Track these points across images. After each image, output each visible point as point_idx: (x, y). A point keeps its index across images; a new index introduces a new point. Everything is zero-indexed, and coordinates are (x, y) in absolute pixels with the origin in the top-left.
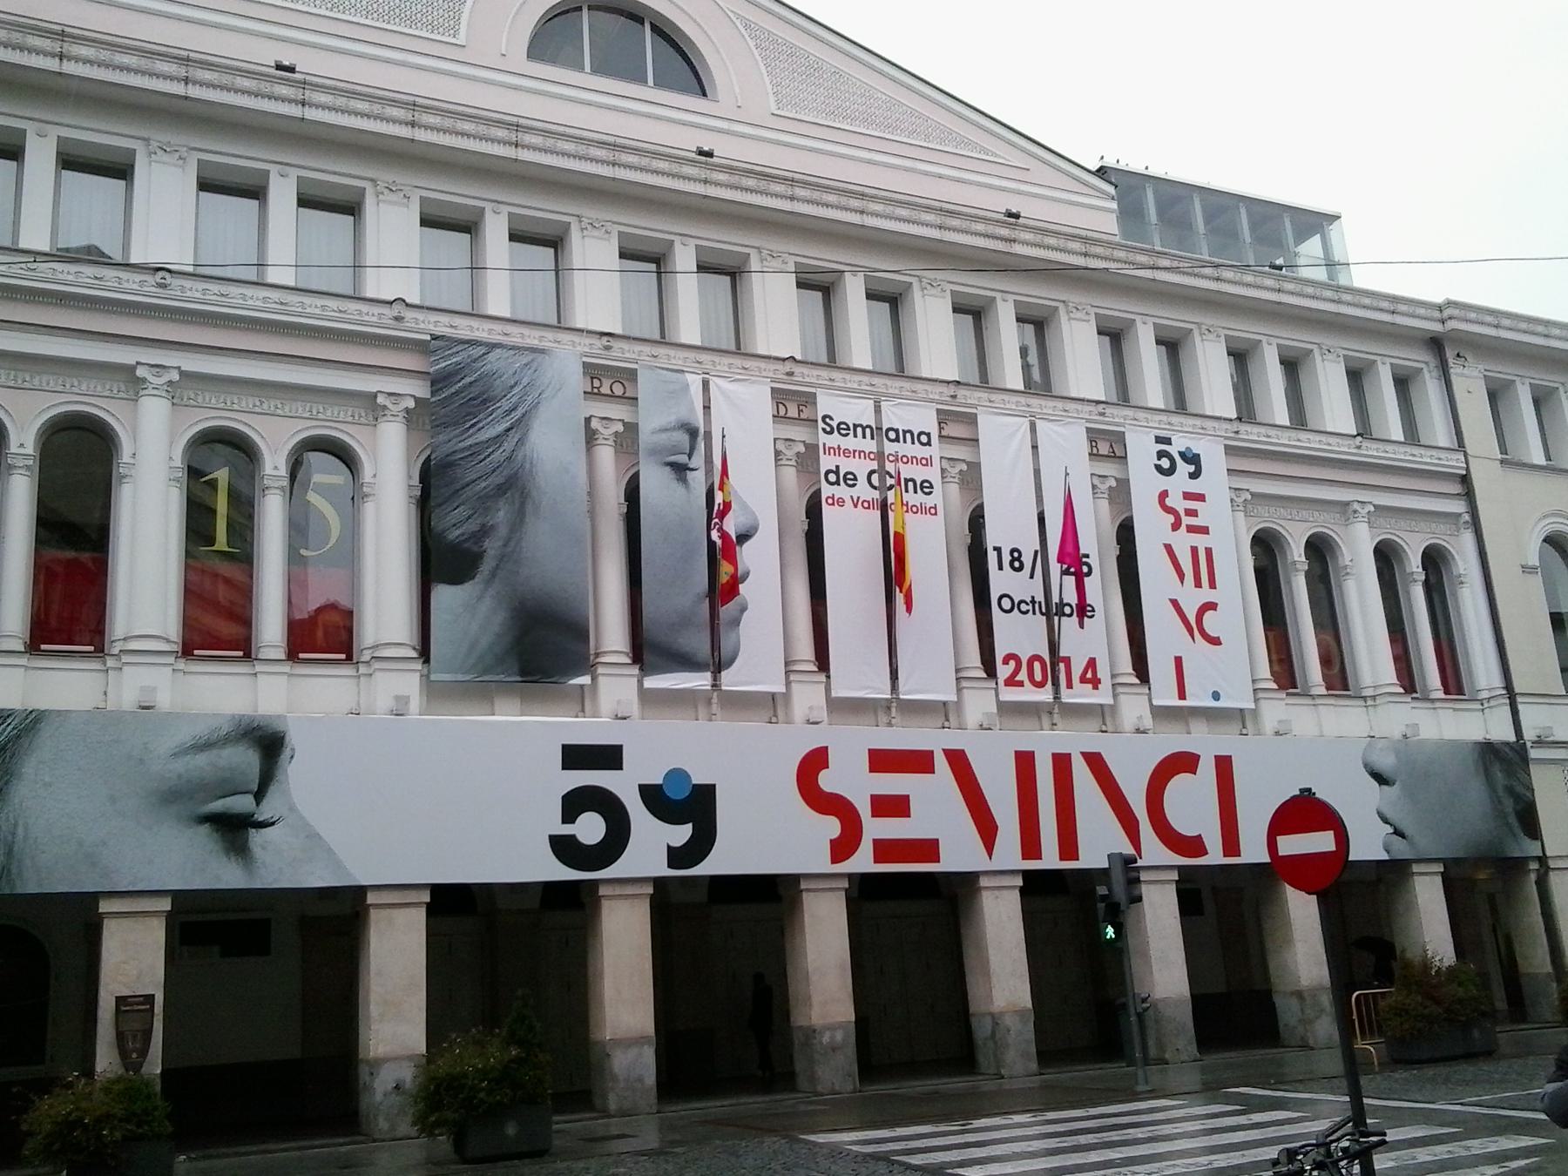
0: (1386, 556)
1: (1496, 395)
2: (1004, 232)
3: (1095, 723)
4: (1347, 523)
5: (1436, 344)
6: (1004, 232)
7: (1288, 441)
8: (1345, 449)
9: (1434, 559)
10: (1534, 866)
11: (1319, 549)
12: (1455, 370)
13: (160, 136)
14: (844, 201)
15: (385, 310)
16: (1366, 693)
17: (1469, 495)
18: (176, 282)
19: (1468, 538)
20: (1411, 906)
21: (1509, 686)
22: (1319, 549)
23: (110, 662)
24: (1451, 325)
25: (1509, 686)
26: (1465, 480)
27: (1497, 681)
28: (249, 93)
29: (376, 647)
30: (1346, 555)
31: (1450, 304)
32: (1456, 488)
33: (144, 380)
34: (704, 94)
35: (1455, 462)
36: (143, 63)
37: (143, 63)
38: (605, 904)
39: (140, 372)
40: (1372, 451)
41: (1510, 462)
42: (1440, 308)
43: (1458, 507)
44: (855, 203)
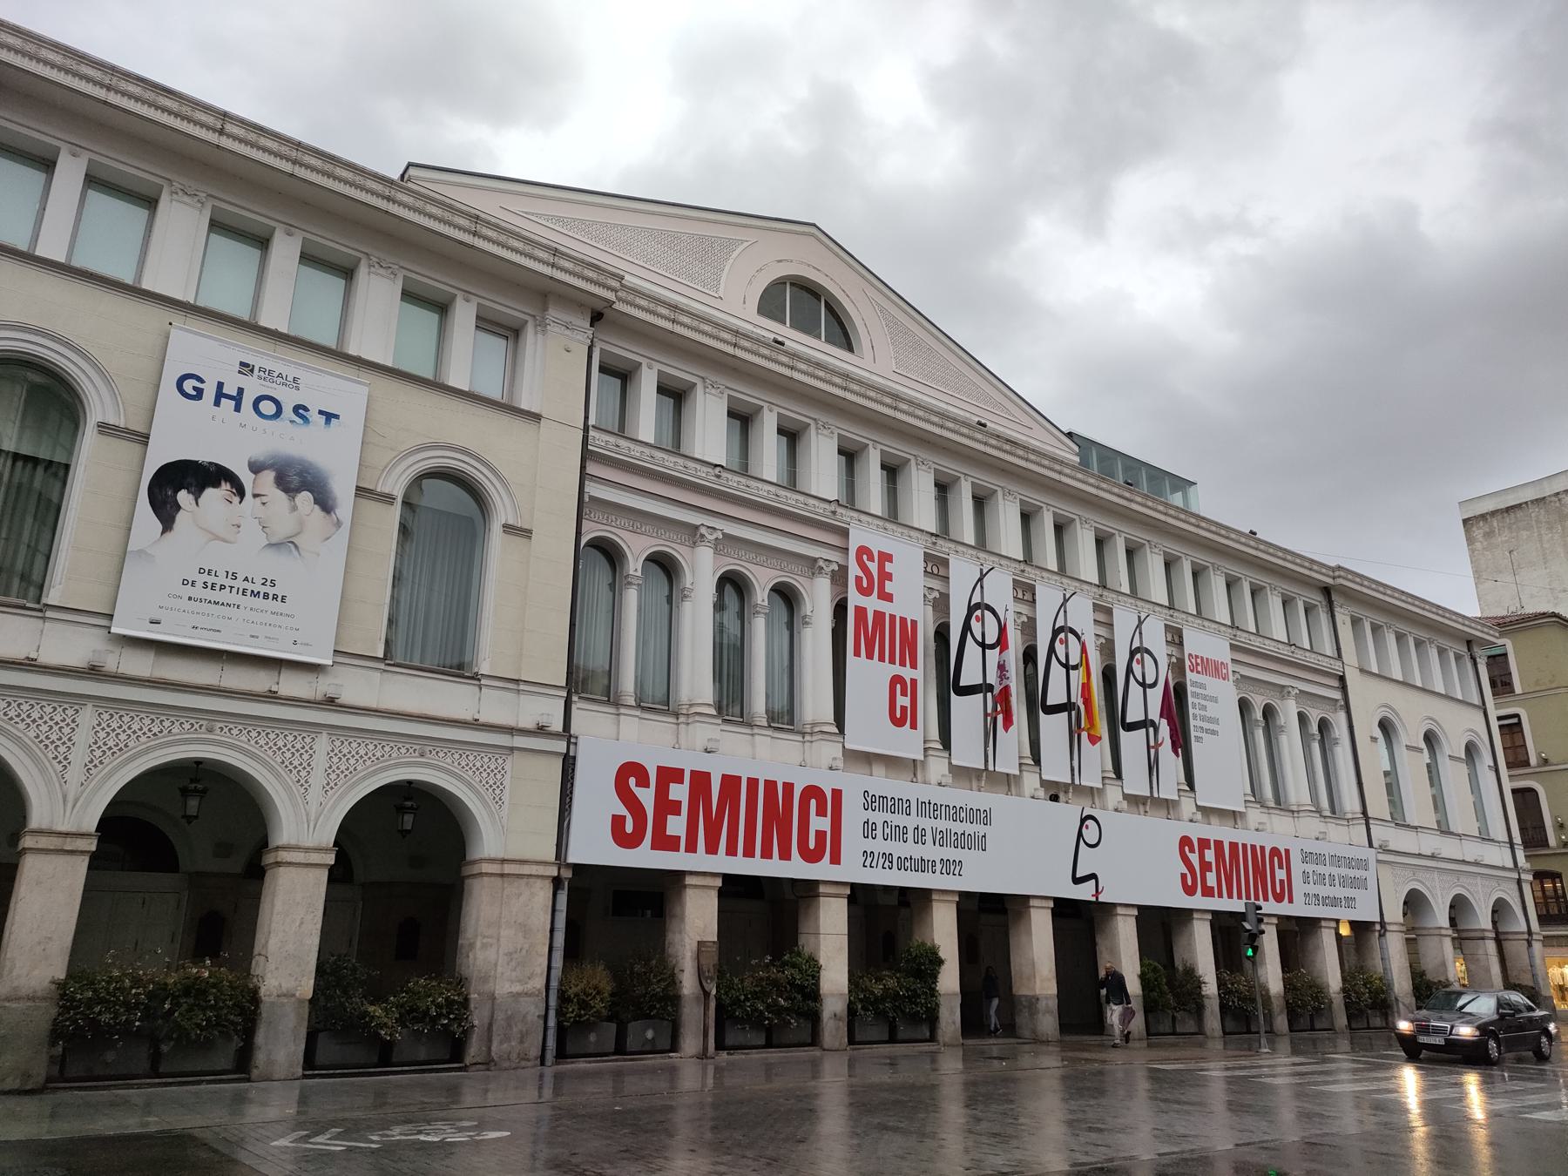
0: (1302, 718)
1: (1356, 622)
2: (1127, 495)
3: (1164, 812)
4: (1283, 698)
5: (1327, 591)
6: (1127, 495)
7: (1257, 643)
8: (1285, 652)
9: (1324, 725)
10: (1378, 927)
11: (1269, 712)
12: (1337, 610)
13: (712, 377)
14: (1052, 465)
15: (826, 506)
16: (1295, 808)
17: (1343, 688)
18: (724, 474)
19: (1342, 715)
20: (1318, 947)
21: (1364, 812)
22: (1269, 712)
23: (682, 719)
24: (1341, 581)
25: (1364, 812)
26: (1342, 679)
27: (1358, 808)
28: (766, 358)
29: (814, 724)
30: (1281, 720)
31: (1339, 568)
32: (1336, 683)
33: (702, 536)
34: (850, 349)
35: (1337, 665)
36: (715, 331)
37: (715, 331)
38: (935, 905)
39: (703, 530)
40: (1299, 656)
41: (1362, 671)
42: (1333, 569)
43: (1337, 695)
44: (1057, 467)
